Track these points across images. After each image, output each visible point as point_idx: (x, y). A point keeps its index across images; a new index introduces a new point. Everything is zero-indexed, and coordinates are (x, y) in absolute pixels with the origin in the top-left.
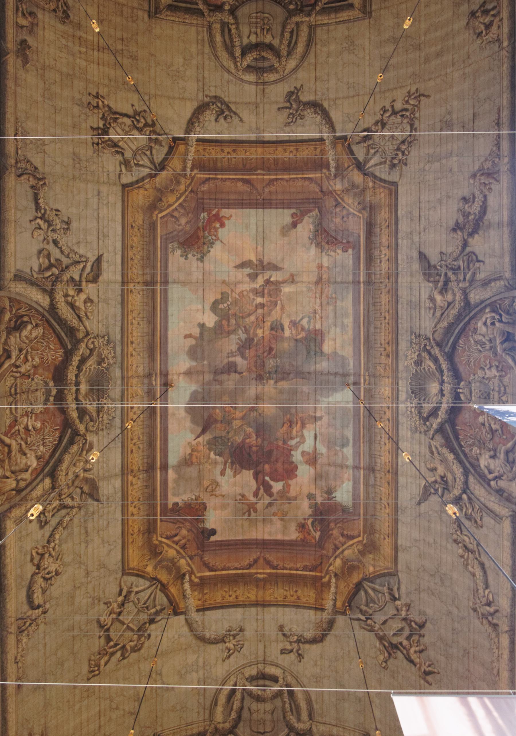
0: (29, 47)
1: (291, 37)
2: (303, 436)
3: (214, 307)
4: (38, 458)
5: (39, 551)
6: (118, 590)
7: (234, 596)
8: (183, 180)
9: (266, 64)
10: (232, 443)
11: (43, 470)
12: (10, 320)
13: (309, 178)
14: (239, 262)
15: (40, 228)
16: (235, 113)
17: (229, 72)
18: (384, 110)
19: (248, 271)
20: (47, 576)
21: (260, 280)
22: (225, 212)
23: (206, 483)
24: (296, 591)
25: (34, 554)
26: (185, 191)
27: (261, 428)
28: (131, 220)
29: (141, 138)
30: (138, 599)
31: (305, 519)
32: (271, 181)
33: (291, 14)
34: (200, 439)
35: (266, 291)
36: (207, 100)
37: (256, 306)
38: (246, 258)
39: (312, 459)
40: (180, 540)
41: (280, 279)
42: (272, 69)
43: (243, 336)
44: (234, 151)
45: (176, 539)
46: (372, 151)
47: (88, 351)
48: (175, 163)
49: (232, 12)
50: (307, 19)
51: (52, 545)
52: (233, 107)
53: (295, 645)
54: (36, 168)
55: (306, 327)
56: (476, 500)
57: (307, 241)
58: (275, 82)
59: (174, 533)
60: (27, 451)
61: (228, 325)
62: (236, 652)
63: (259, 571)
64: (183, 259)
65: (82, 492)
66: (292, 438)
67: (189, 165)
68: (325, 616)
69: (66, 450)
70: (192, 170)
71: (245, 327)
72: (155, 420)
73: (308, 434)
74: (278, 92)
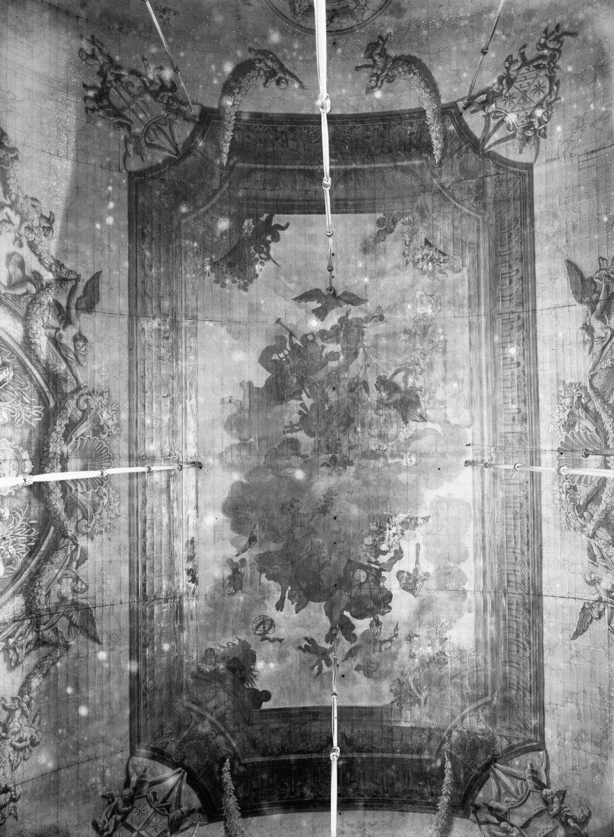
5: (7, 705)
6: (124, 778)
14: (299, 293)
16: (292, 75)
18: (510, 60)
19: (315, 305)
20: (18, 745)
22: (278, 219)
30: (154, 794)
36: (251, 56)
38: (312, 285)
46: (493, 122)
47: (80, 413)
52: (287, 66)
55: (402, 385)
65: (72, 624)
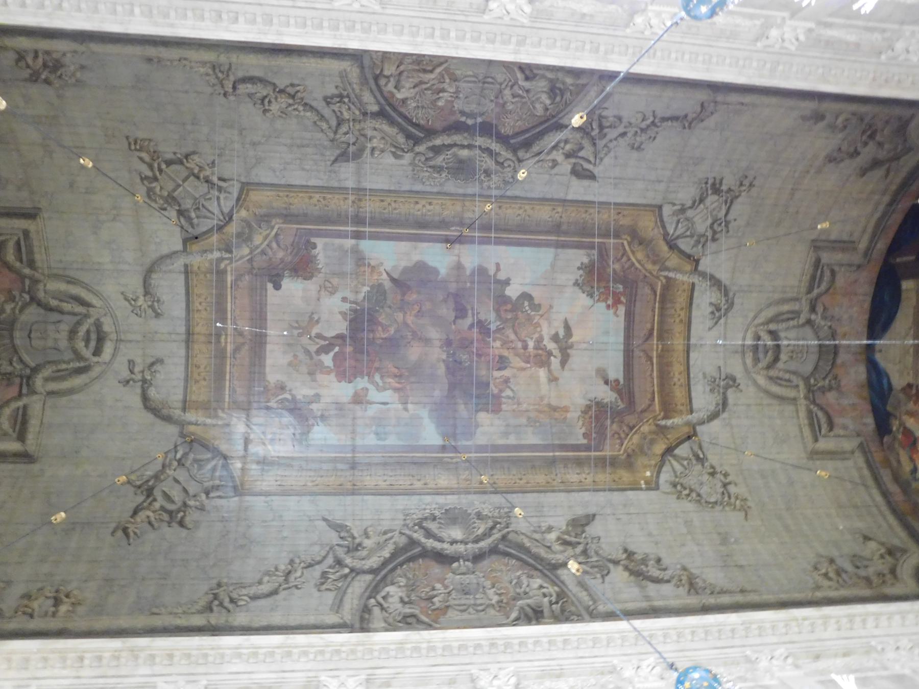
0: (815, 124)
1: (786, 380)
2: (385, 389)
3: (526, 296)
4: (404, 101)
5: (299, 94)
7: (200, 308)
8: (657, 267)
9: (761, 356)
10: (377, 311)
11: (390, 105)
12: (564, 83)
13: (654, 398)
14: (571, 323)
15: (643, 120)
16: (716, 323)
17: (755, 317)
19: (562, 333)
21: (551, 346)
22: (622, 310)
23: (335, 281)
24: (205, 379)
25: (298, 88)
26: (646, 270)
27: (393, 344)
28: (625, 213)
29: (702, 226)
31: (290, 390)
32: (650, 359)
33: (806, 380)
34: (385, 276)
35: (540, 352)
36: (731, 295)
37: (524, 341)
39: (359, 399)
40: (271, 249)
41: (553, 367)
42: (756, 360)
43: (493, 327)
44: (681, 321)
45: (274, 245)
47: (502, 161)
48: (674, 260)
49: (809, 322)
50: (802, 396)
51: (301, 108)
52: (722, 321)
53: (139, 377)
54: (702, 121)
55: (503, 395)
56: (347, 583)
57: (592, 396)
58: (744, 364)
59: (281, 243)
60: (417, 89)
61: (506, 310)
62: (131, 308)
63: (229, 337)
64: (579, 265)
66: (382, 377)
67: (671, 275)
68: (177, 413)
69: (402, 130)
70: (666, 277)
71: (503, 328)
72: (413, 228)
73: (388, 395)
74: (736, 367)
